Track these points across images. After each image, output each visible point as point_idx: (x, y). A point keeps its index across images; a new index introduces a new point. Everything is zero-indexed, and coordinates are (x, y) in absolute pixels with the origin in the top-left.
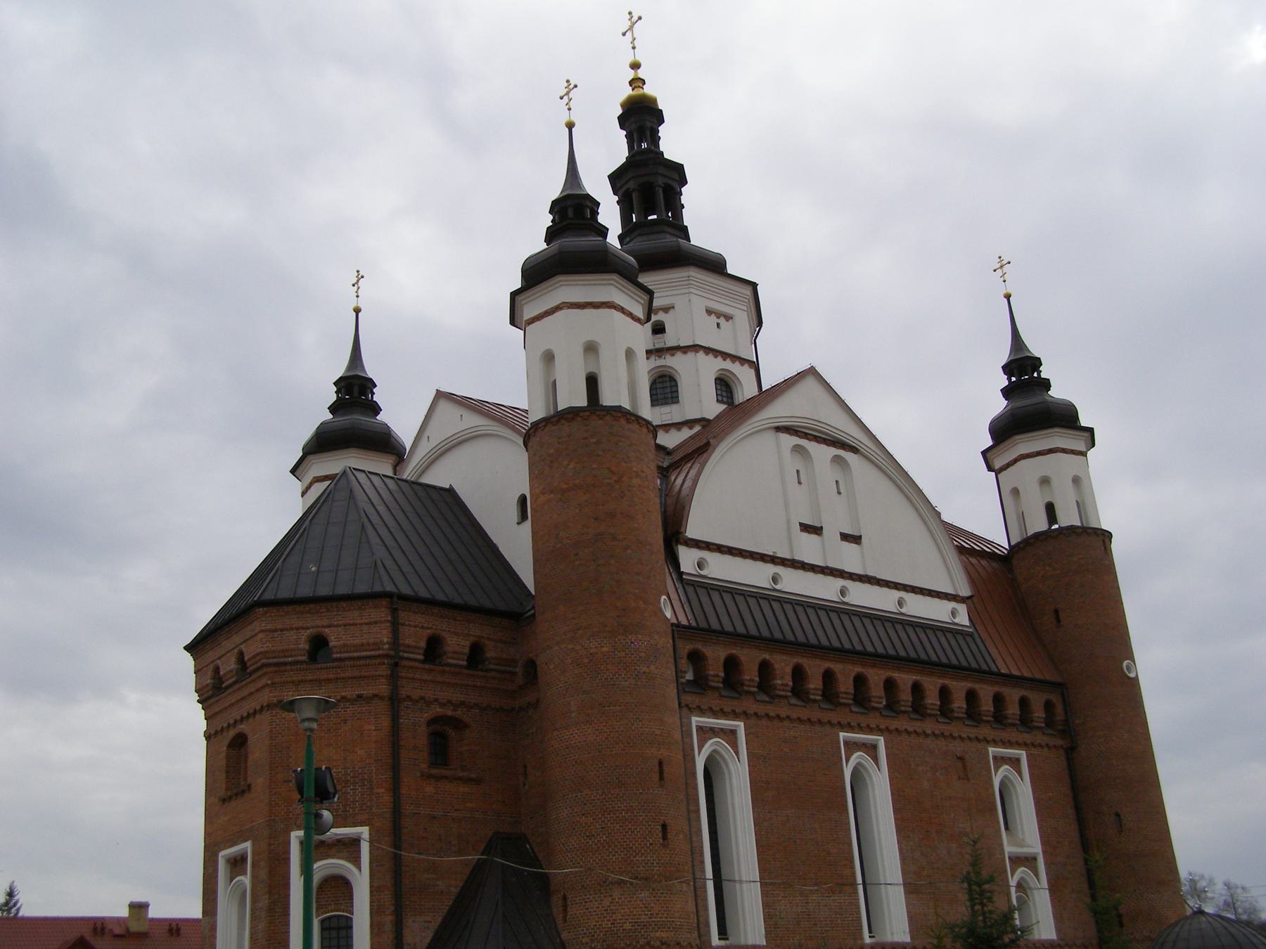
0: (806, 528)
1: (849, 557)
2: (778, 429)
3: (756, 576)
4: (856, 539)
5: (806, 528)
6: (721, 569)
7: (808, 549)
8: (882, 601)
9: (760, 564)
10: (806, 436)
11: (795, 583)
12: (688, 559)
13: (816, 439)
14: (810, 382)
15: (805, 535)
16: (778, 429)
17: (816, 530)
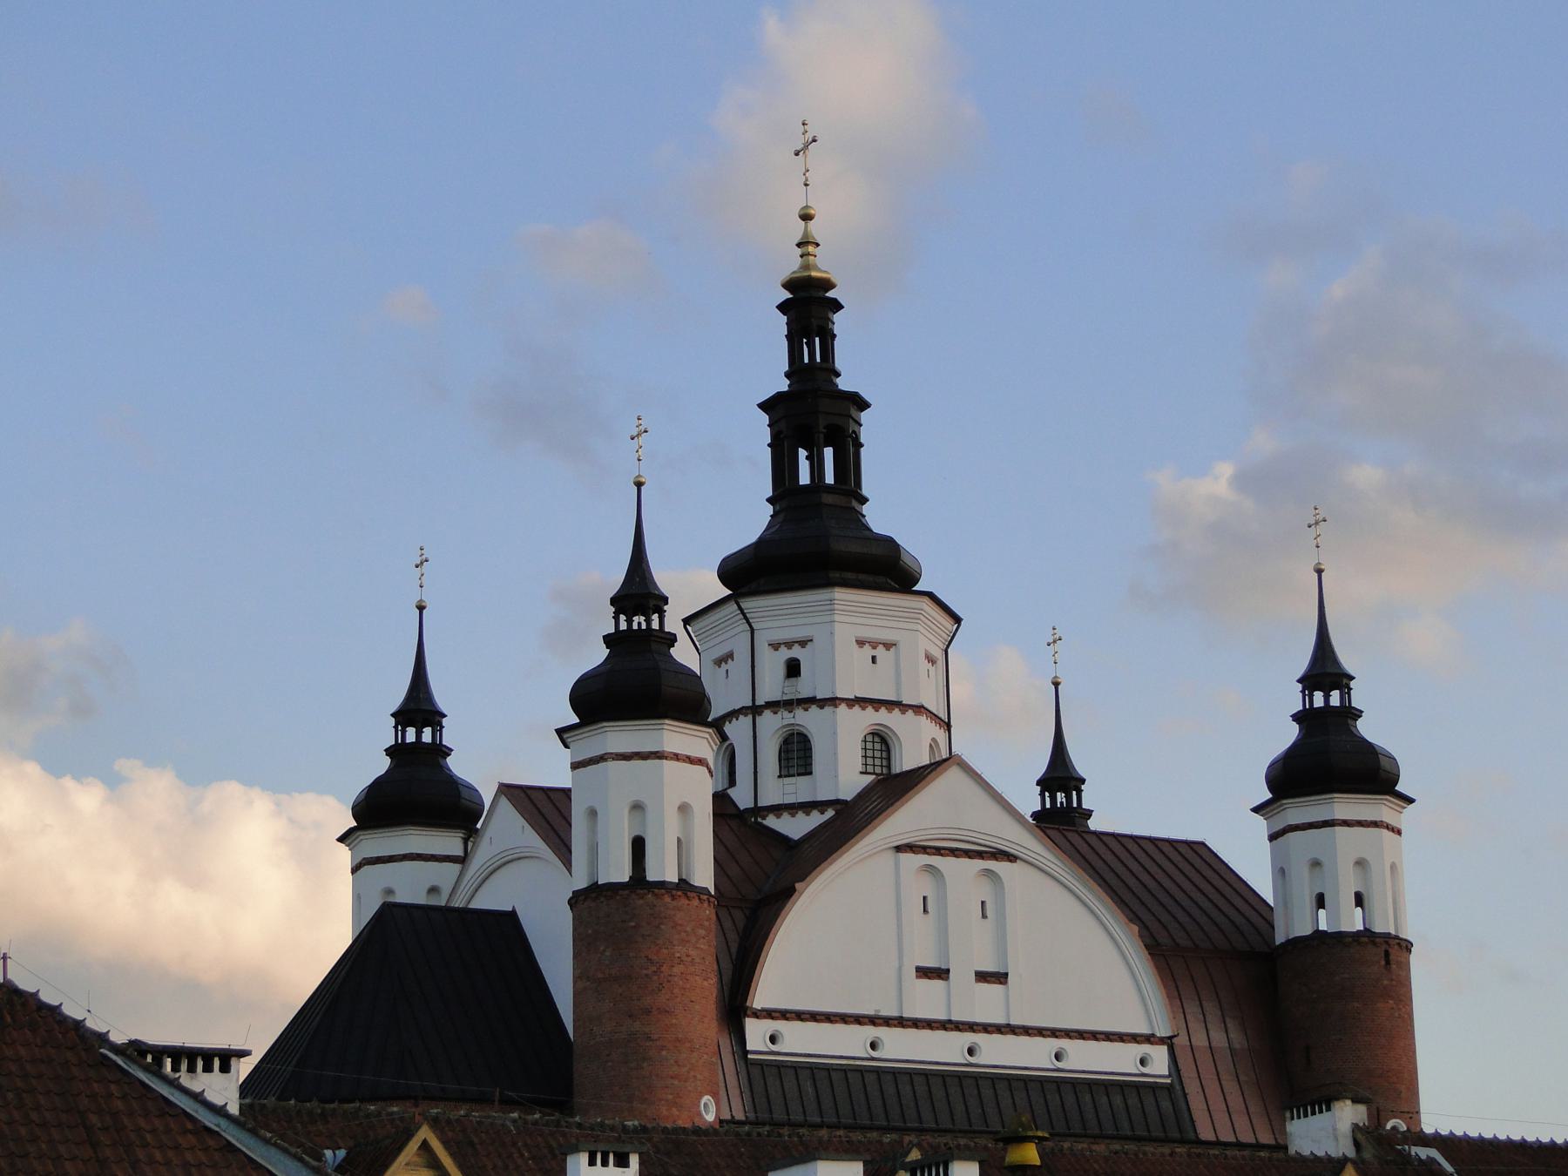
0: (924, 973)
1: (986, 1004)
2: (899, 849)
3: (845, 1044)
4: (1000, 978)
5: (924, 973)
6: (801, 1041)
7: (927, 1000)
8: (1031, 1056)
9: (855, 1028)
10: (938, 851)
11: (901, 1048)
12: (756, 1034)
13: (954, 852)
14: (951, 778)
15: (925, 982)
16: (899, 849)
17: (941, 974)
